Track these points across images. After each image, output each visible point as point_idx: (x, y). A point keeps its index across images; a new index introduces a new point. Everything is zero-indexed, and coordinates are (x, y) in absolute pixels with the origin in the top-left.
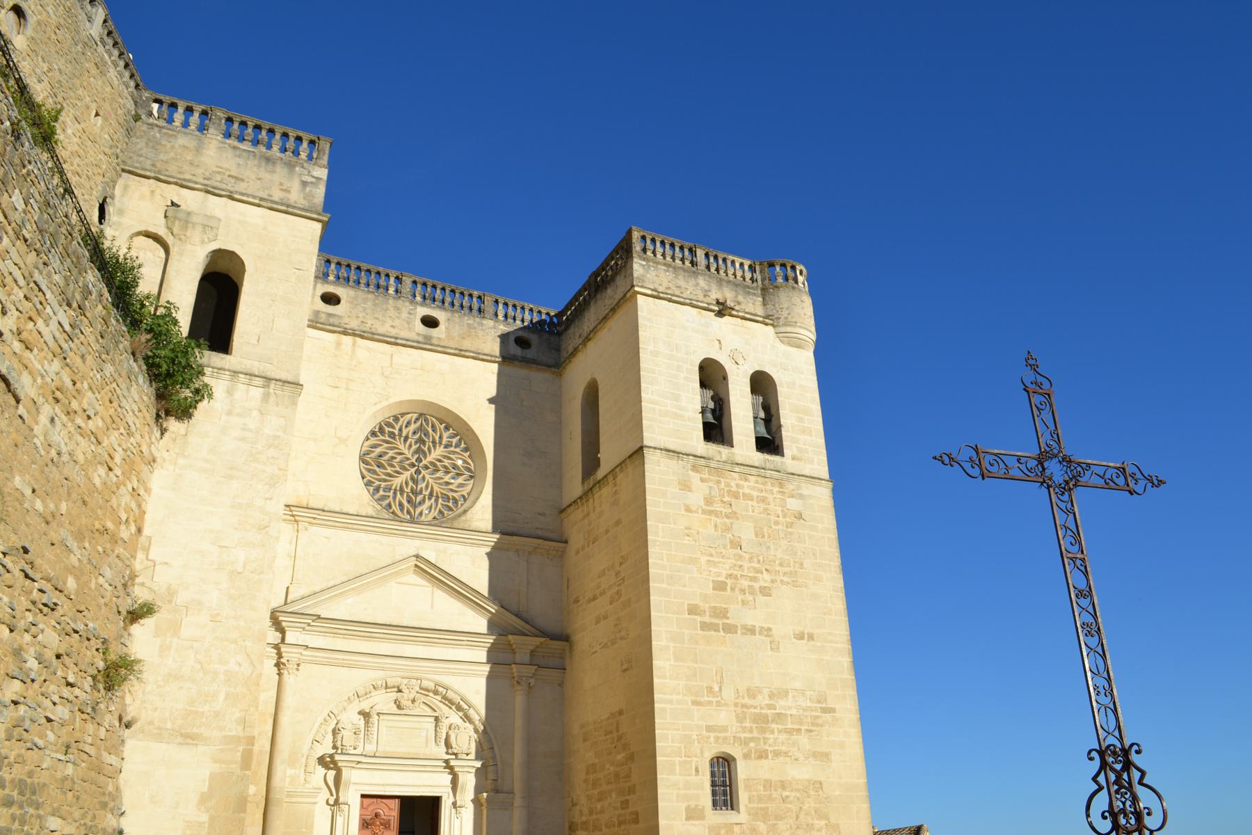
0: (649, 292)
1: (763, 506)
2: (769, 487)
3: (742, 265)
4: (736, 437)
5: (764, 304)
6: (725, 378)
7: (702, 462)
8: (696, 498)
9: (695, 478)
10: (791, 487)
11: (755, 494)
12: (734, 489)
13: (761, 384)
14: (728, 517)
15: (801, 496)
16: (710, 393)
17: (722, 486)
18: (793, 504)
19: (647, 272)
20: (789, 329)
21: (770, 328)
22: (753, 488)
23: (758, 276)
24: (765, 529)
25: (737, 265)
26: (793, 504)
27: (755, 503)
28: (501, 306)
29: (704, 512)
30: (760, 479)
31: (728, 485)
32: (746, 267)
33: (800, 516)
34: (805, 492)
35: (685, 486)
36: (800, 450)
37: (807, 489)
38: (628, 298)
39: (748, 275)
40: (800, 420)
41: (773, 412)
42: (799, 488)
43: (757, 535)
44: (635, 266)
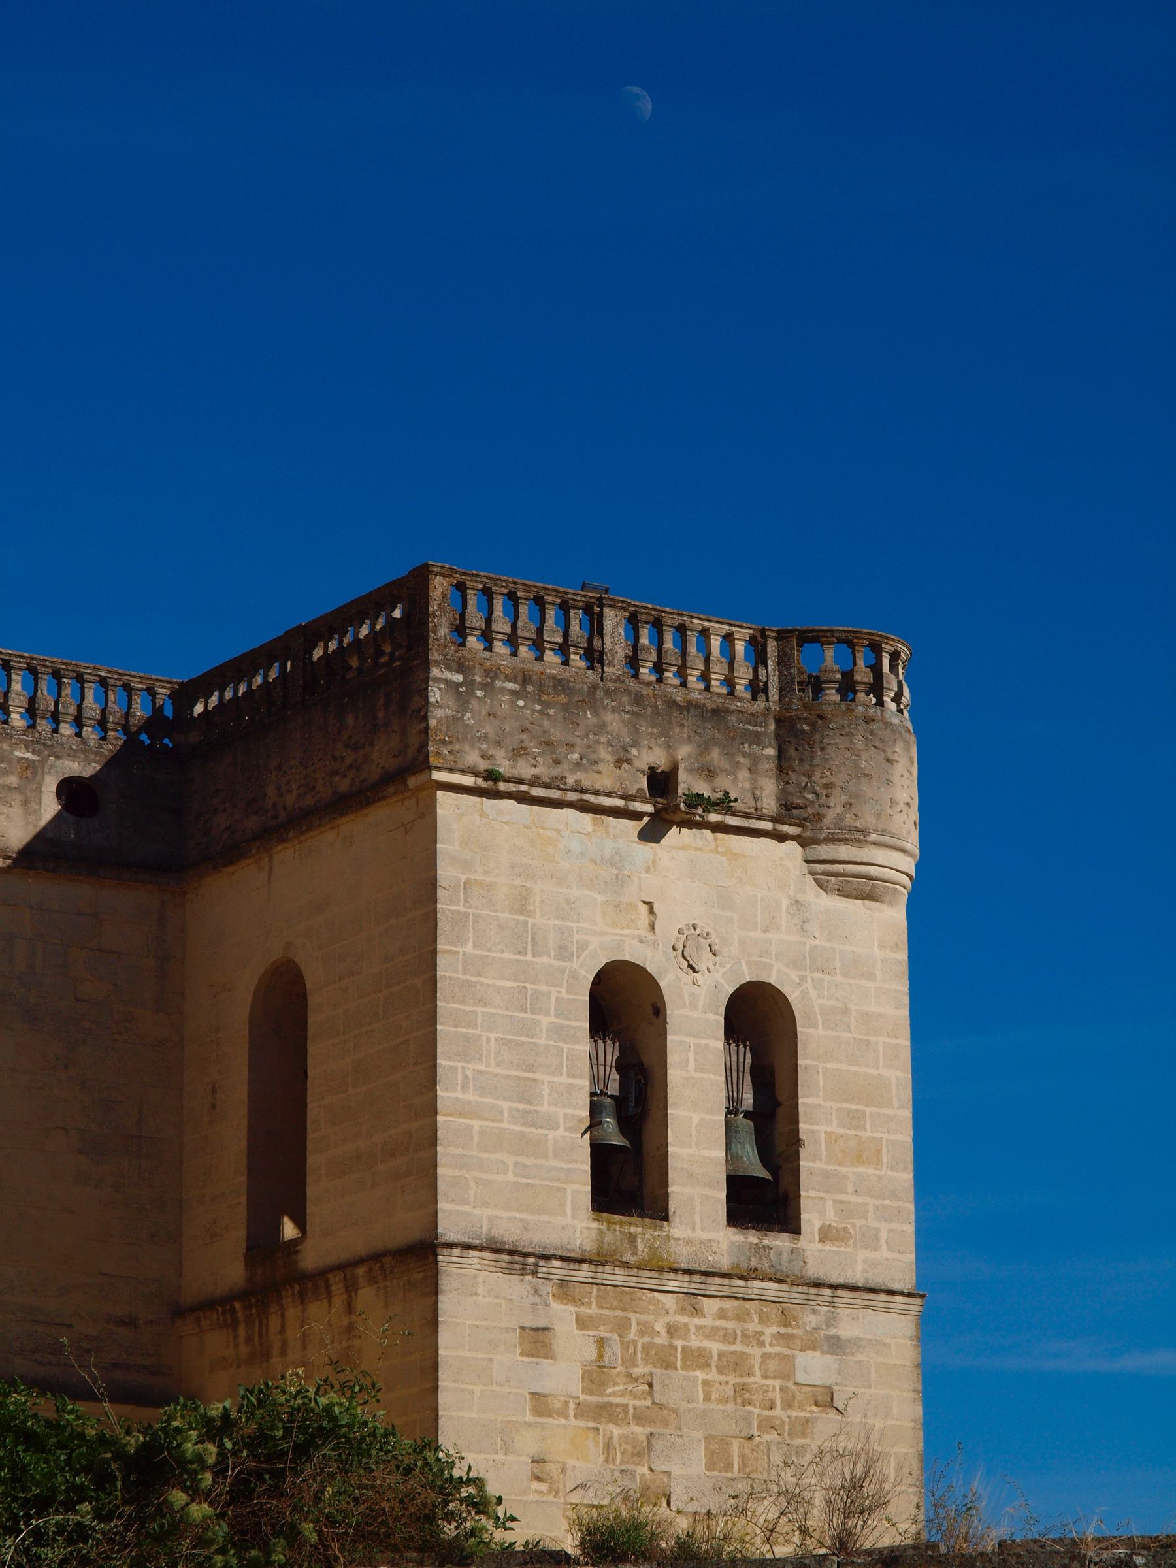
0: (468, 780)
1: (733, 1379)
2: (753, 1326)
3: (728, 638)
4: (678, 1190)
5: (783, 767)
6: (658, 1010)
7: (584, 1272)
8: (563, 1376)
9: (562, 1315)
10: (811, 1320)
11: (715, 1347)
12: (662, 1340)
13: (757, 1019)
14: (640, 1418)
15: (836, 1346)
16: (611, 1051)
17: (632, 1334)
18: (814, 1367)
19: (469, 705)
20: (844, 851)
21: (791, 845)
22: (712, 1333)
23: (771, 675)
24: (735, 1445)
25: (716, 642)
26: (814, 1367)
27: (713, 1375)
28: (16, 678)
29: (582, 1411)
30: (728, 1304)
31: (646, 1329)
32: (740, 647)
33: (827, 1400)
34: (846, 1330)
35: (537, 1340)
36: (843, 1209)
37: (854, 1322)
38: (405, 776)
39: (743, 673)
40: (855, 1120)
41: (782, 1094)
42: (831, 1321)
43: (711, 1466)
44: (435, 694)
